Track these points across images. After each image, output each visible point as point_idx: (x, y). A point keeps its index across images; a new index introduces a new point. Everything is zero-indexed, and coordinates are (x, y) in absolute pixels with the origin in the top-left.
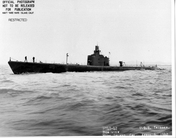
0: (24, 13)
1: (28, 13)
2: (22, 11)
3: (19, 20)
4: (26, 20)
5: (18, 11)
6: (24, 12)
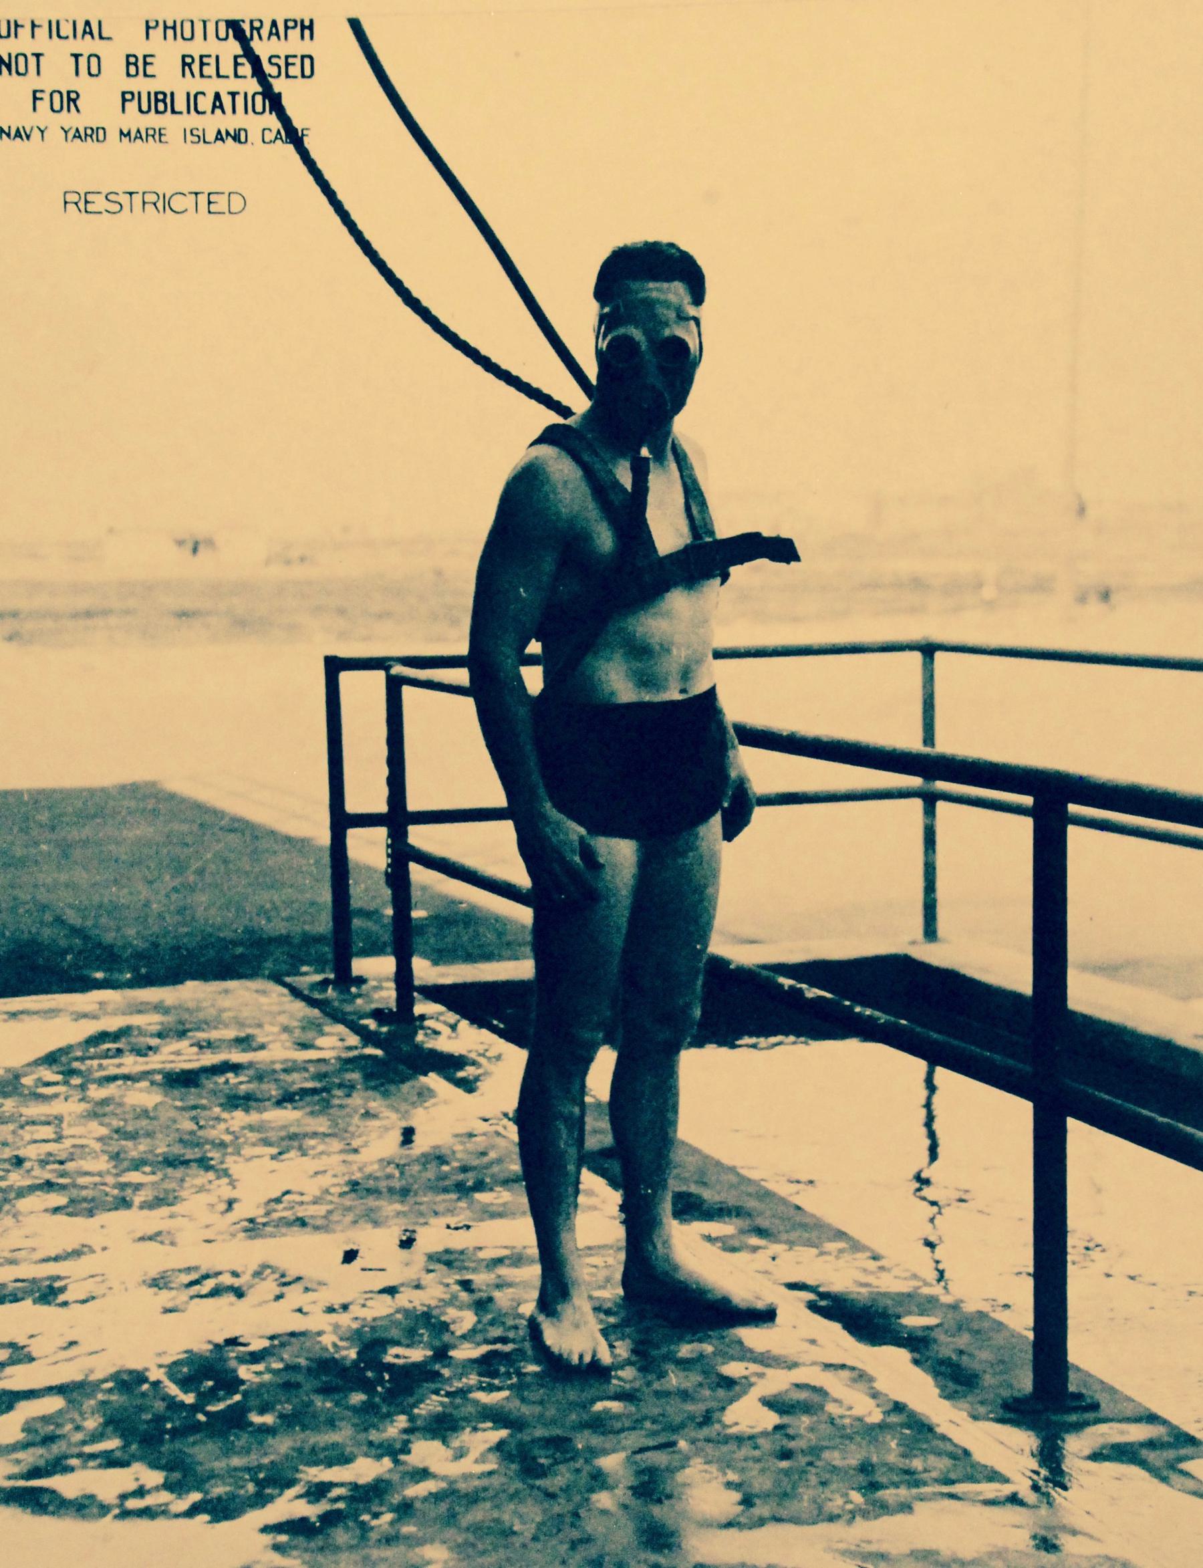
0: (211, 136)
1: (254, 135)
2: (193, 120)
3: (164, 203)
4: (237, 203)
5: (153, 120)
6: (212, 123)
